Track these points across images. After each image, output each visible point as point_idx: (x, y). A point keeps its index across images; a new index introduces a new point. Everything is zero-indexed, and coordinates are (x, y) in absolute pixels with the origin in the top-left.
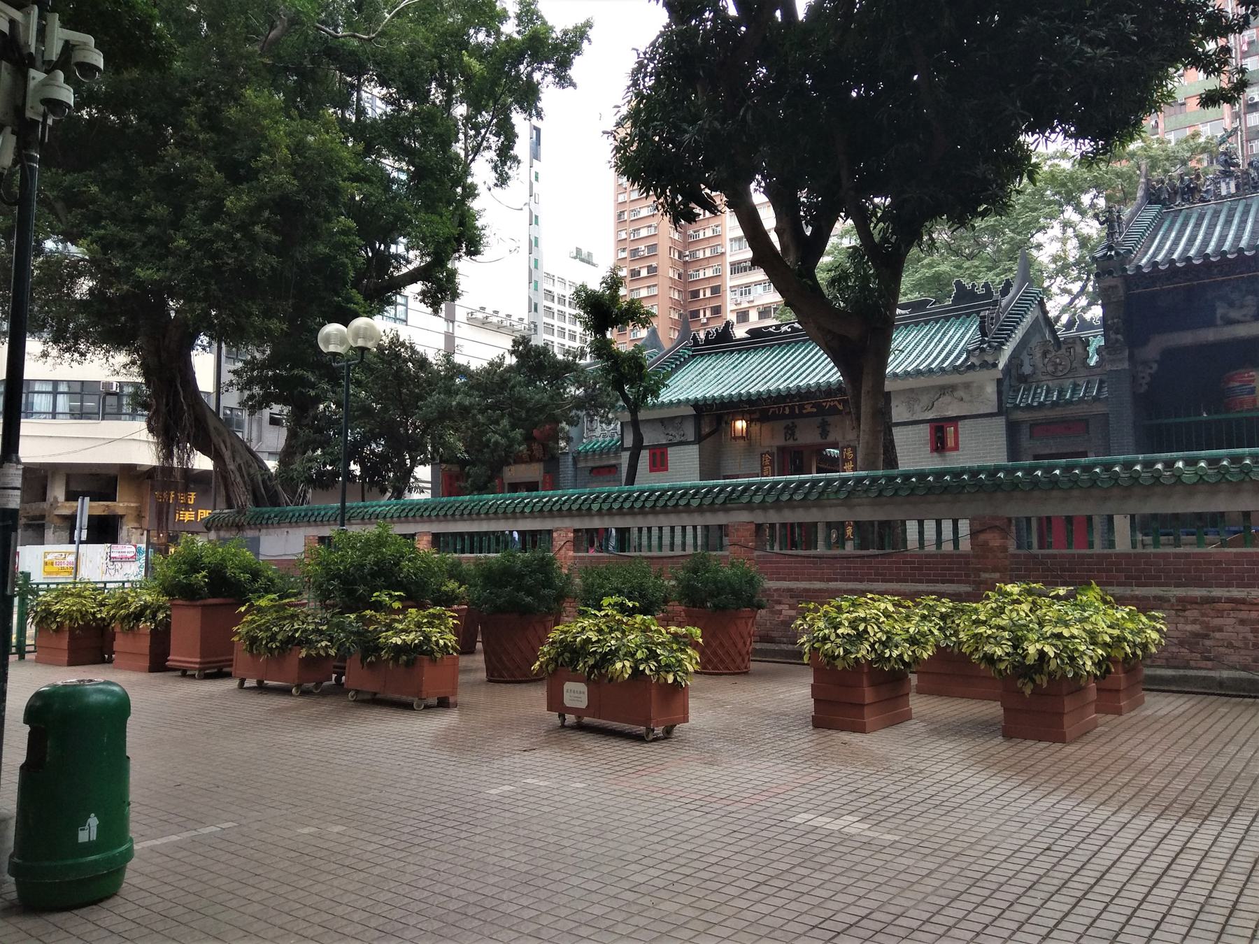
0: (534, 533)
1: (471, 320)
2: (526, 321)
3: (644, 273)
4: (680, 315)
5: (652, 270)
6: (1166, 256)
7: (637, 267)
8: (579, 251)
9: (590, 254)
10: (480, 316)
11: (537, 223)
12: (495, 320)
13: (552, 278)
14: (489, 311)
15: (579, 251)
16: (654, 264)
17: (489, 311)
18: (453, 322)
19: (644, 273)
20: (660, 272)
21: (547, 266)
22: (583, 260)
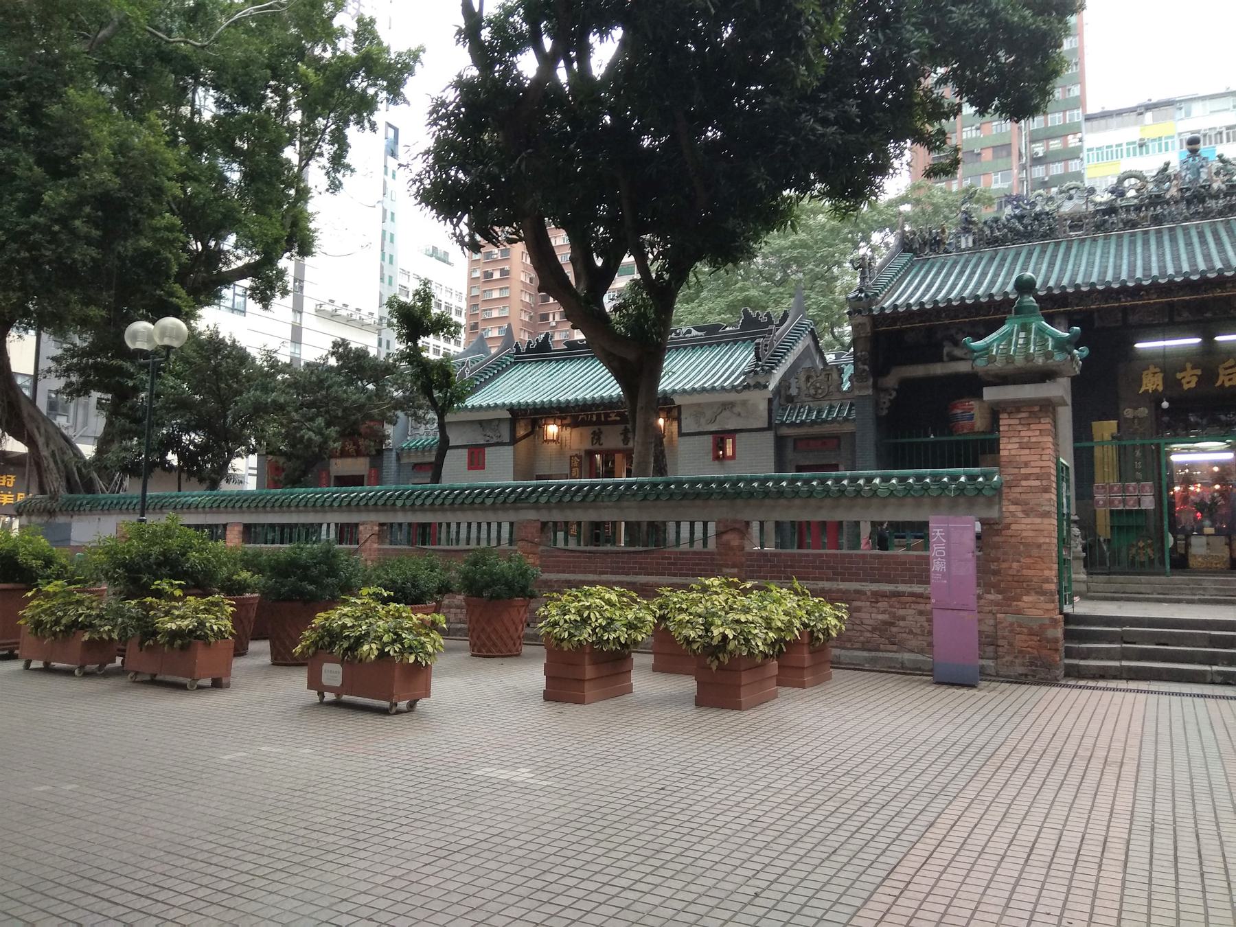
0: (424, 526)
1: (319, 312)
2: (376, 316)
3: (497, 275)
4: (531, 318)
5: (504, 273)
6: (959, 293)
7: (490, 270)
8: (435, 249)
9: (446, 254)
10: (329, 308)
11: (393, 219)
12: (344, 313)
13: (408, 274)
14: (338, 304)
15: (435, 249)
16: (507, 268)
17: (338, 304)
18: (301, 313)
19: (497, 275)
20: (513, 274)
21: (402, 261)
22: (438, 259)
